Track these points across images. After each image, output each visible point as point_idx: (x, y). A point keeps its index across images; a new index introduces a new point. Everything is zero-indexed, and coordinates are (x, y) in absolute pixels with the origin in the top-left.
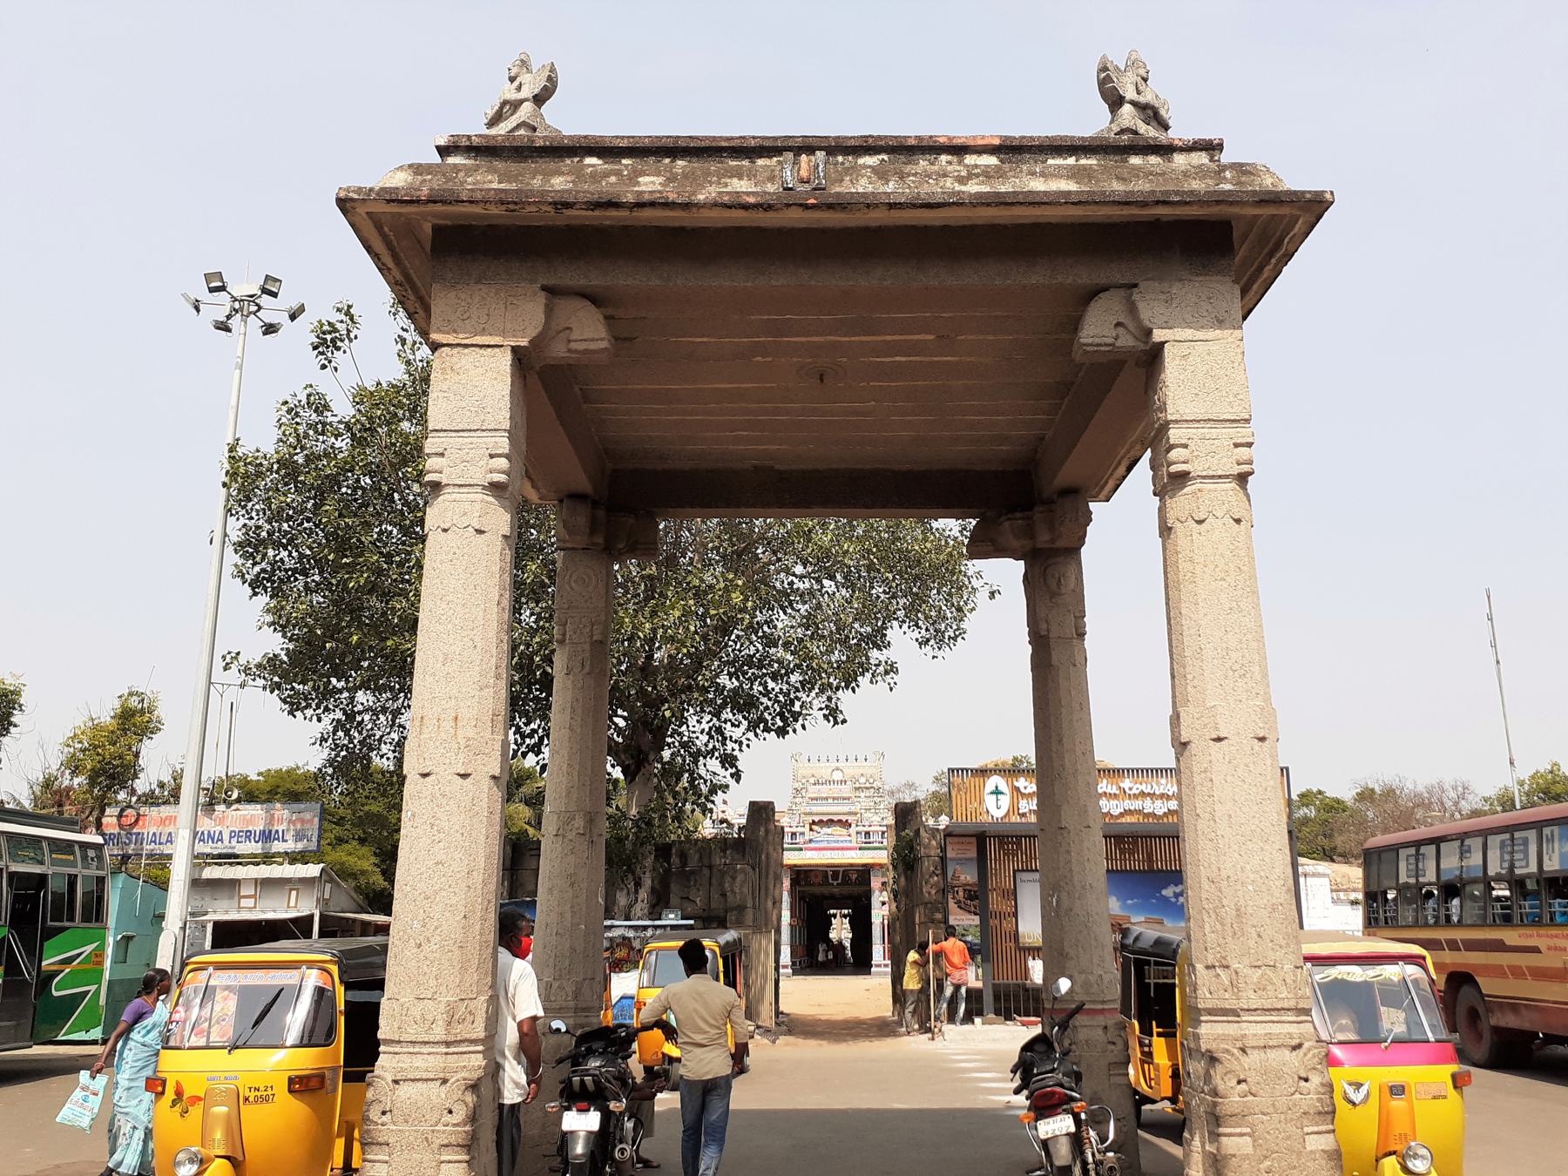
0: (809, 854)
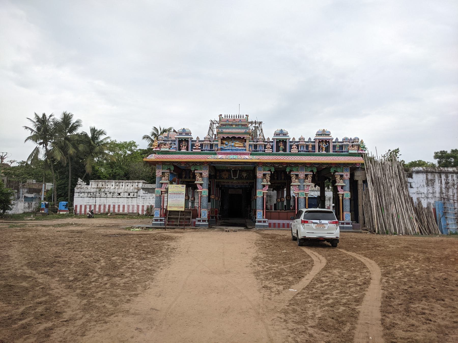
0: (220, 156)
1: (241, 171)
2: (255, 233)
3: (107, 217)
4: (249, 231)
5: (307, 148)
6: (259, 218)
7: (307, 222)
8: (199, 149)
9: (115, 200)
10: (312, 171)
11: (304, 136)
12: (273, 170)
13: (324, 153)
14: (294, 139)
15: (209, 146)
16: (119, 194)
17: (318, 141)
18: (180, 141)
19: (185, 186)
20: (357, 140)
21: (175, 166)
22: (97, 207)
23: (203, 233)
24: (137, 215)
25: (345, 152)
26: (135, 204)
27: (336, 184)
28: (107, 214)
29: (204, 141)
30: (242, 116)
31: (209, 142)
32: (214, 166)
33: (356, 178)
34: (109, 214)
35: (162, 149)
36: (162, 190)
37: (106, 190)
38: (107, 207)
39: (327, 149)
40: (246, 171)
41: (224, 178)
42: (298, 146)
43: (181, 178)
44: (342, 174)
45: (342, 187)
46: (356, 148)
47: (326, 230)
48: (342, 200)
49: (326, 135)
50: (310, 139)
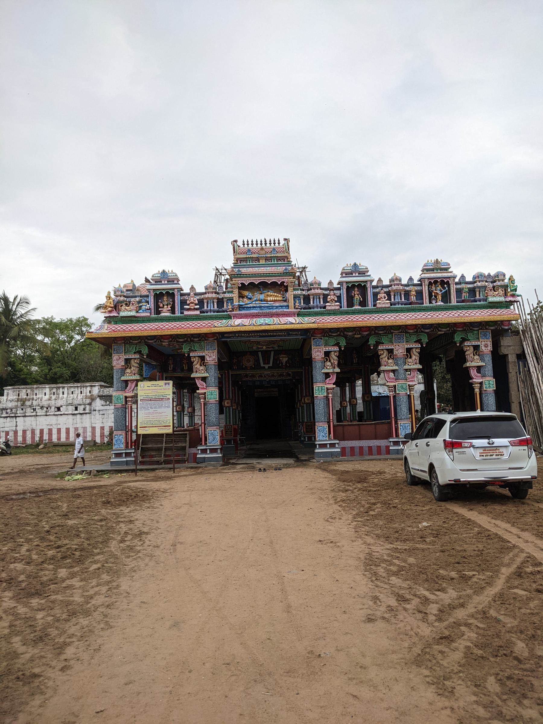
0: (238, 321)
1: (278, 353)
2: (319, 471)
3: (37, 452)
4: (305, 465)
5: (406, 296)
6: (321, 438)
7: (459, 445)
8: (197, 309)
9: (52, 420)
10: (419, 341)
11: (399, 275)
12: (343, 343)
13: (440, 305)
14: (380, 280)
15: (216, 302)
16: (59, 409)
17: (427, 282)
18: (159, 296)
19: (171, 382)
20: (501, 277)
21: (150, 347)
22: (20, 433)
23: (212, 477)
24: (92, 444)
25: (480, 301)
26: (88, 425)
27: (468, 364)
28: (38, 445)
29: (205, 293)
30: (277, 242)
31: (214, 295)
32: (226, 342)
33: (504, 351)
34: (41, 446)
35: (122, 314)
36: (127, 395)
37: (35, 403)
38: (38, 433)
39: (446, 297)
41: (246, 368)
42: (388, 294)
44: (476, 343)
45: (479, 369)
46: (501, 291)
47: (506, 461)
48: (481, 394)
49: (441, 269)
50: (411, 279)
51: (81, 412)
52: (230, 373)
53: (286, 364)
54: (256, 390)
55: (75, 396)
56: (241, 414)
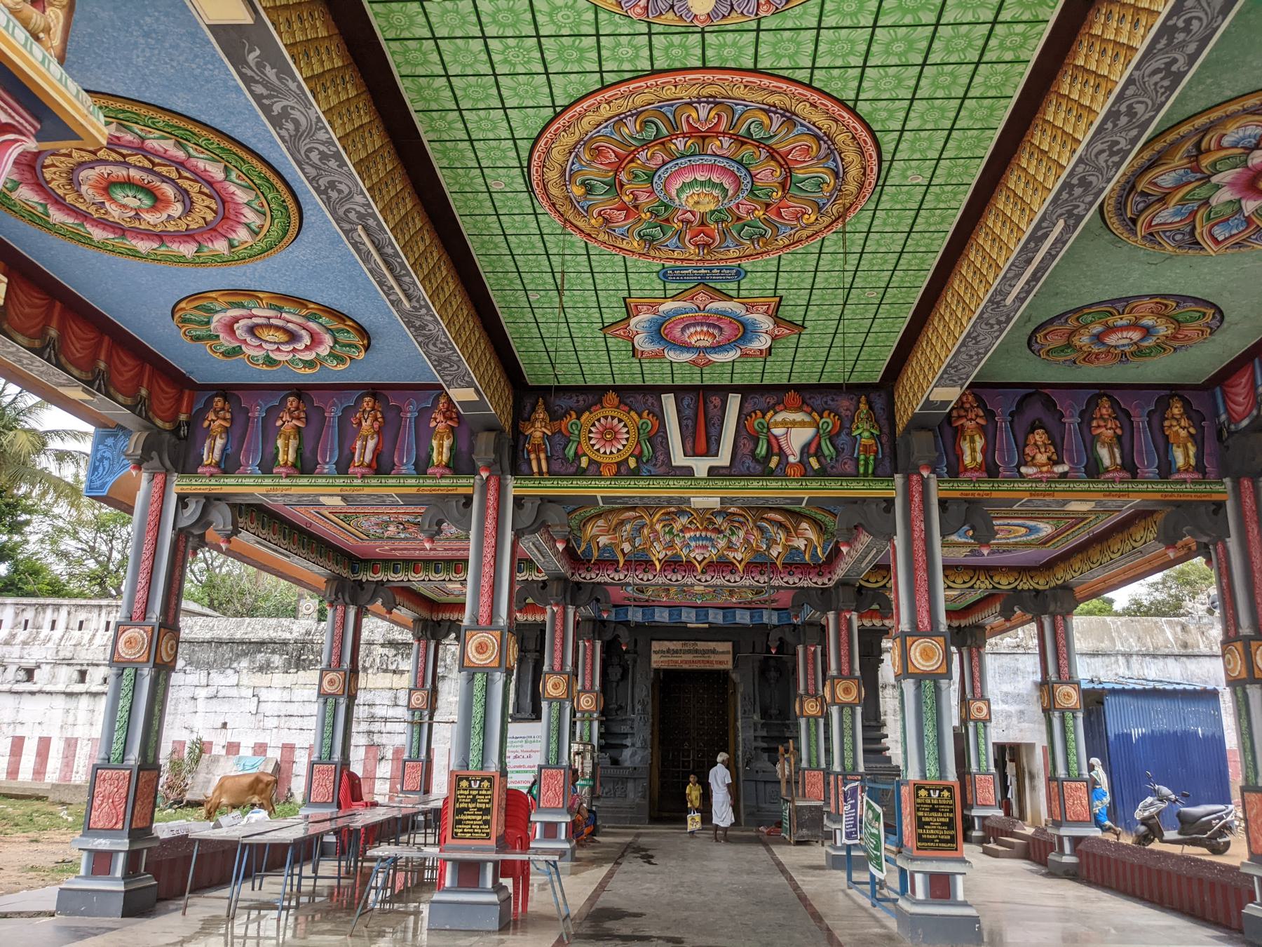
40: (807, 395)
41: (595, 470)
43: (185, 462)
51: (94, 689)
52: (511, 492)
53: (803, 462)
54: (656, 646)
55: (86, 635)
56: (596, 724)
